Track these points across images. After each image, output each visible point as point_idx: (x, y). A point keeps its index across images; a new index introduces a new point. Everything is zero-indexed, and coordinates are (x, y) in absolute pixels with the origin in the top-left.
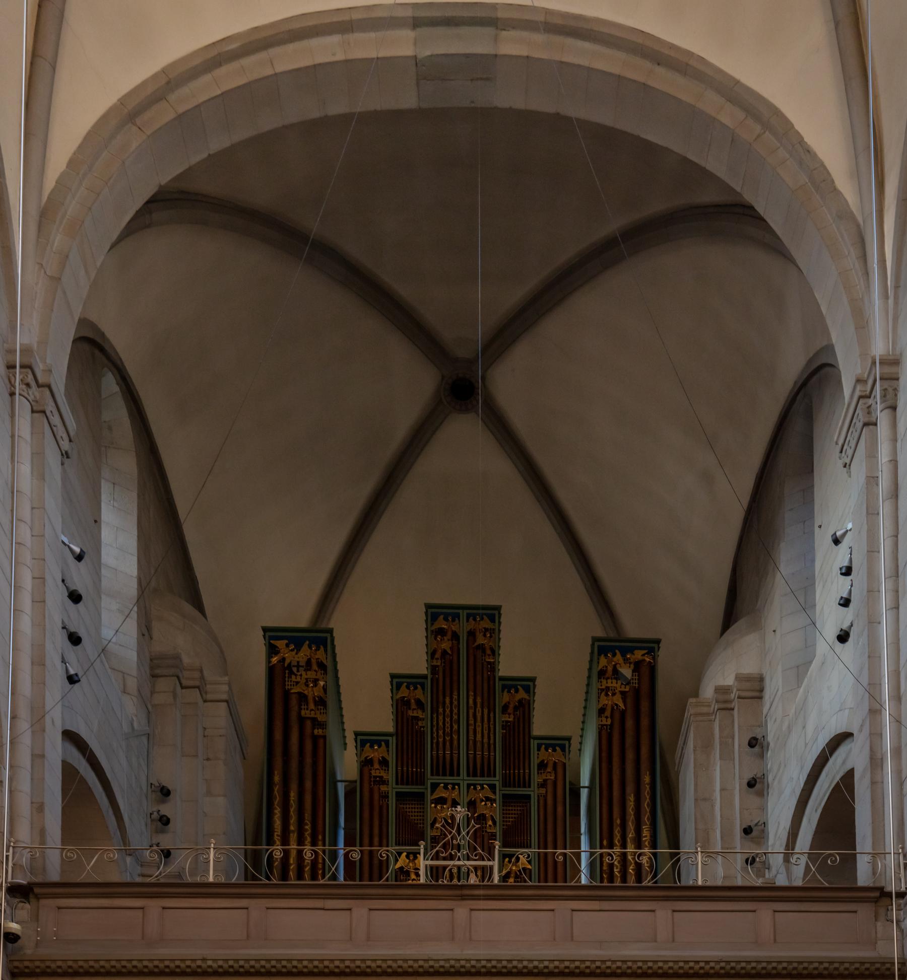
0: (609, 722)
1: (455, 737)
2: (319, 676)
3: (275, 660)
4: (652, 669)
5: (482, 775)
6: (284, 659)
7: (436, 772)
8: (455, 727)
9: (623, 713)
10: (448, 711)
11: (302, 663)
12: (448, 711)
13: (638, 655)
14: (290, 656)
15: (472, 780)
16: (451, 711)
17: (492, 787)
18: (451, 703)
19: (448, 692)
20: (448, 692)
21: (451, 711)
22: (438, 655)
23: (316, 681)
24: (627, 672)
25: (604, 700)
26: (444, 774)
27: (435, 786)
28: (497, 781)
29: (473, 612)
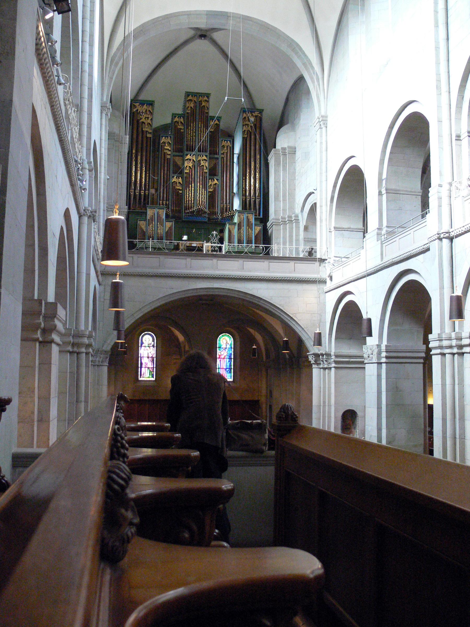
0: (246, 136)
1: (194, 138)
2: (150, 116)
3: (135, 110)
4: (261, 119)
5: (203, 152)
6: (137, 110)
7: (187, 150)
8: (194, 134)
9: (251, 133)
10: (192, 128)
11: (144, 111)
12: (192, 128)
13: (256, 113)
14: (140, 109)
15: (199, 153)
16: (193, 129)
17: (206, 156)
18: (193, 126)
19: (192, 121)
20: (192, 121)
21: (193, 129)
22: (189, 109)
23: (148, 118)
24: (252, 119)
25: (245, 128)
26: (190, 151)
27: (187, 155)
28: (208, 154)
29: (202, 95)
